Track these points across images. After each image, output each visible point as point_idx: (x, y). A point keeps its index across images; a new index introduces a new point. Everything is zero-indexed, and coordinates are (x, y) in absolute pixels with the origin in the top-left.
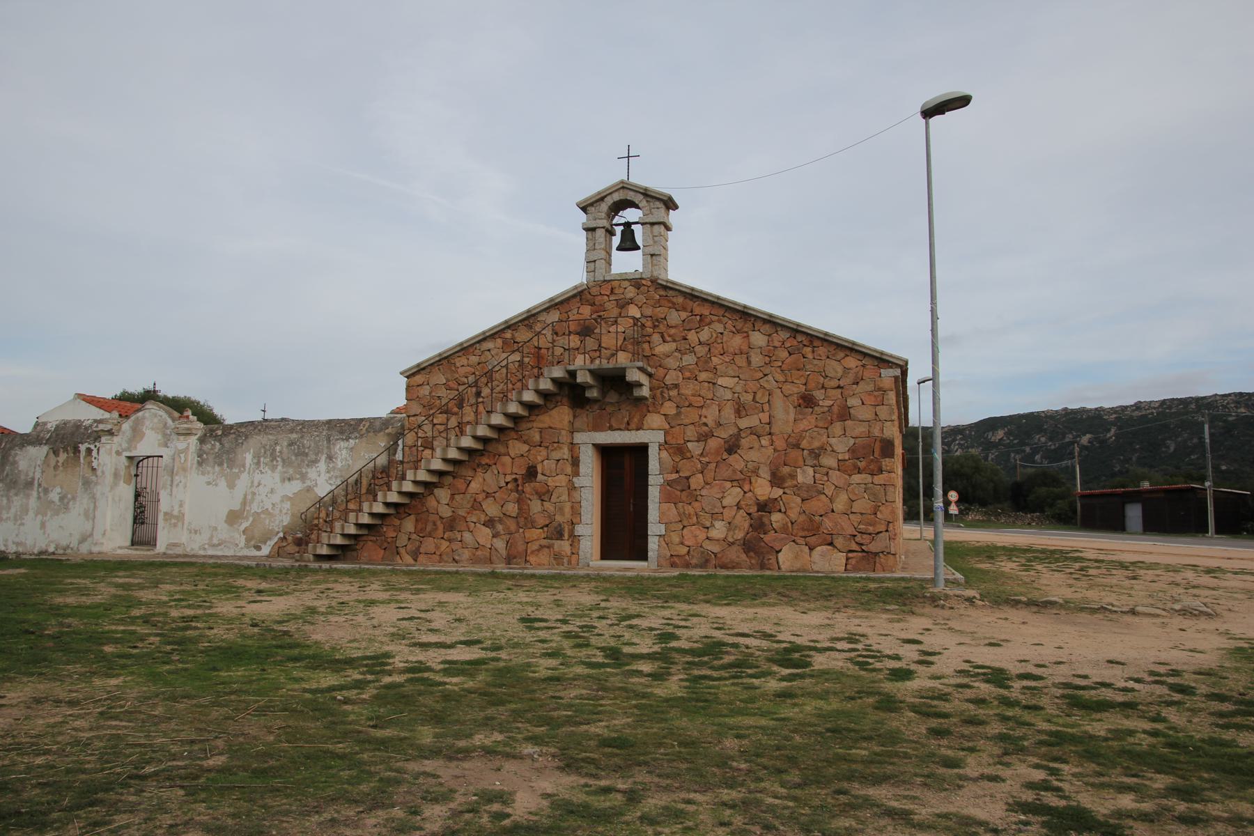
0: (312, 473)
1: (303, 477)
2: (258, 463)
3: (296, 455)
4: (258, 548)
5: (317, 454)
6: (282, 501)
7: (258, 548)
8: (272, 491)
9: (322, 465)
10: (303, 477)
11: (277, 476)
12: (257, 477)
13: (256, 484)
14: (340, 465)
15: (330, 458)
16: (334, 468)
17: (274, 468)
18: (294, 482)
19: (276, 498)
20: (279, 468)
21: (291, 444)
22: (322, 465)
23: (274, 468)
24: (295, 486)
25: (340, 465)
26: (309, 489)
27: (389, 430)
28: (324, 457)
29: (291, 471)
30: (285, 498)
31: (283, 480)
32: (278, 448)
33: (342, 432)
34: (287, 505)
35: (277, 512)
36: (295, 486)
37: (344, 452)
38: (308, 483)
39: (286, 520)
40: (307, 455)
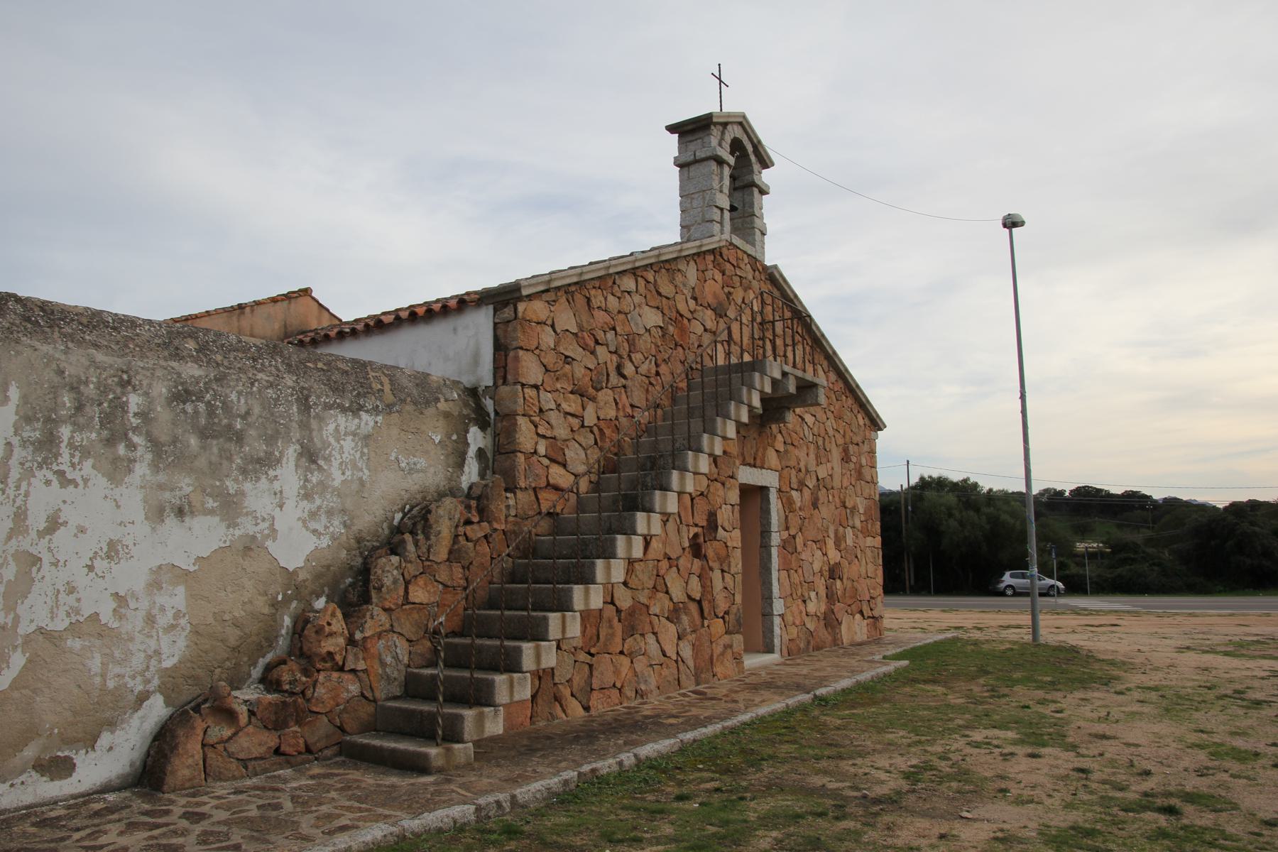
0: (257, 497)
1: (230, 507)
2: (48, 444)
3: (205, 434)
4: (59, 767)
5: (271, 440)
6: (155, 585)
7: (59, 767)
8: (113, 551)
9: (288, 475)
10: (230, 507)
11: (132, 498)
12: (43, 497)
13: (37, 520)
14: (338, 478)
15: (310, 456)
16: (323, 486)
17: (118, 470)
18: (199, 523)
19: (131, 575)
20: (141, 469)
21: (182, 395)
22: (288, 475)
23: (118, 470)
24: (203, 537)
25: (338, 478)
26: (250, 547)
27: (442, 405)
28: (291, 452)
29: (186, 484)
30: (161, 577)
31: (157, 514)
32: (134, 401)
33: (337, 389)
34: (176, 599)
35: (135, 622)
36: (203, 537)
37: (348, 443)
38: (247, 527)
39: (173, 650)
40: (239, 438)
